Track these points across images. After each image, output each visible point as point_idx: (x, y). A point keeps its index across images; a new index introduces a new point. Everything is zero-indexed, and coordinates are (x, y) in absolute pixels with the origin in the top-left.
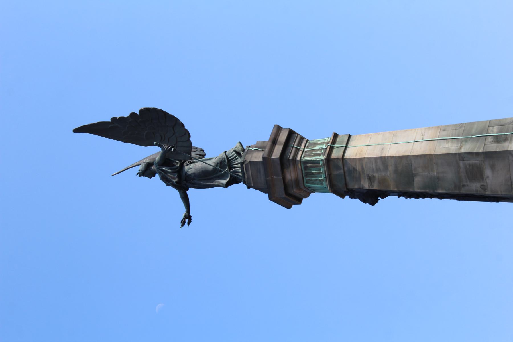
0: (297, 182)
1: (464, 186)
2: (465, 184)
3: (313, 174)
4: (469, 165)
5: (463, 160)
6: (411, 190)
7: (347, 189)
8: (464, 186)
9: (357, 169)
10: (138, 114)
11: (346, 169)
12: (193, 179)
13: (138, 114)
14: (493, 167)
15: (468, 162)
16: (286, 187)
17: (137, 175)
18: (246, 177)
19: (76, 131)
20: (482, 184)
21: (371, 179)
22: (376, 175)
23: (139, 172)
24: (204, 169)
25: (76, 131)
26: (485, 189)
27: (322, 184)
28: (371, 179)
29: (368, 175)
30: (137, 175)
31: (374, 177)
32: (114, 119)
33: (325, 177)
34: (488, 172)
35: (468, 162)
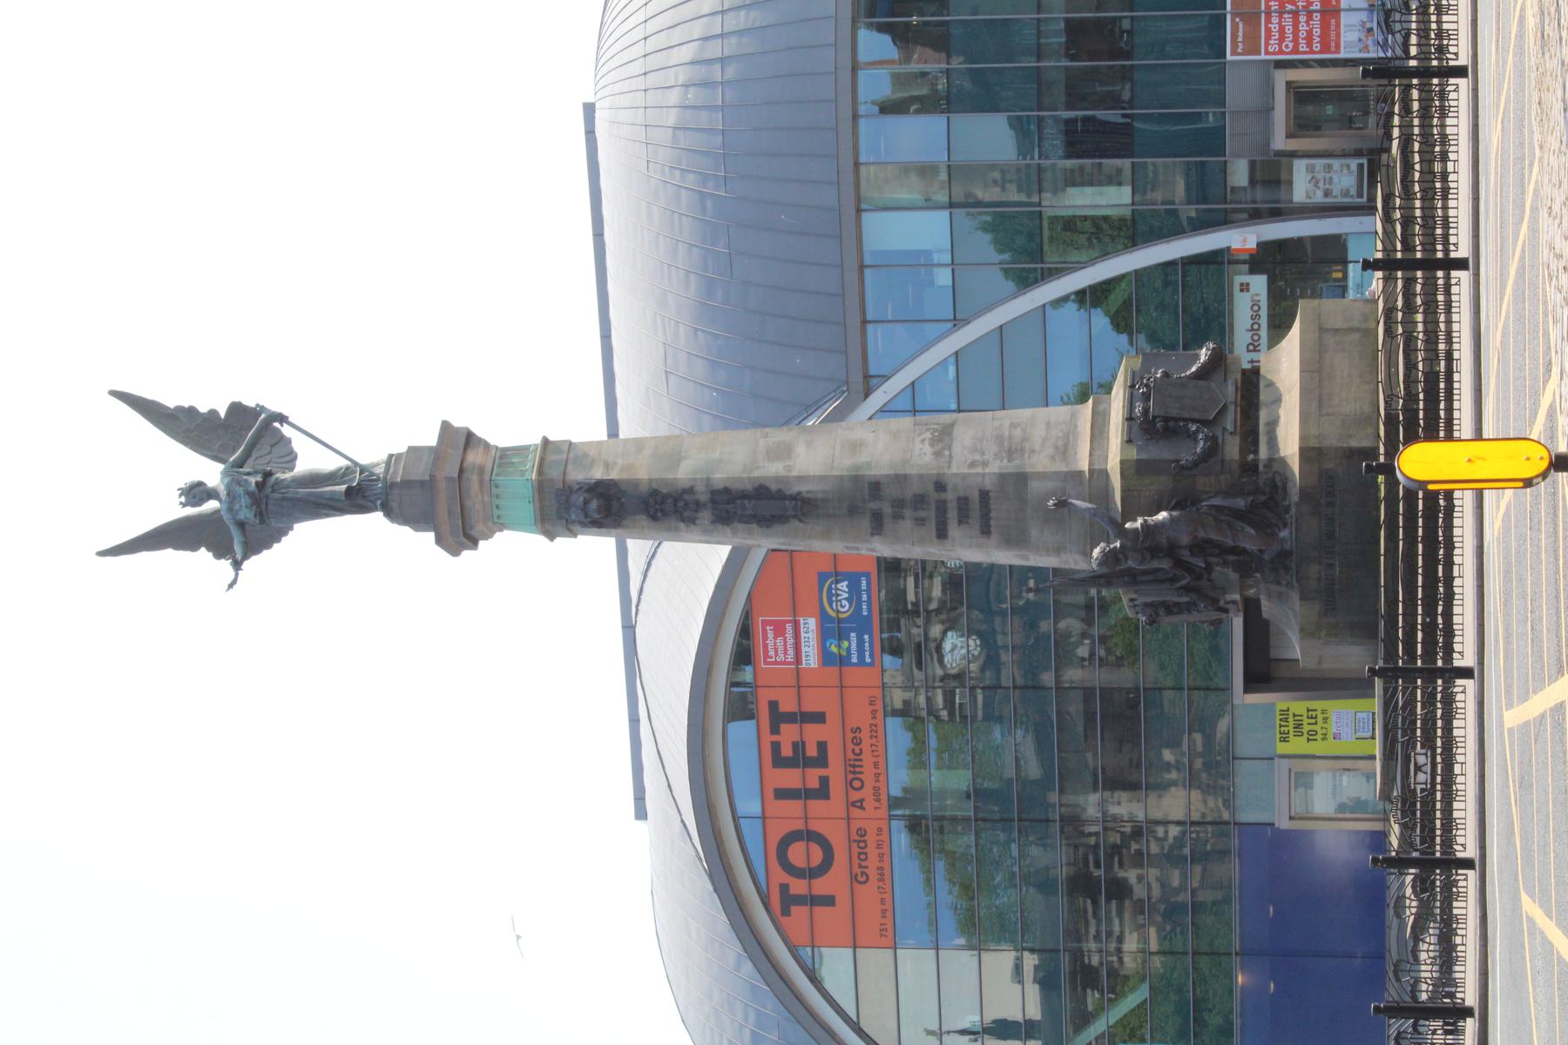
0: (481, 470)
1: (758, 468)
2: (761, 465)
3: (513, 463)
4: (774, 442)
5: (766, 437)
6: (672, 476)
7: (564, 481)
8: (758, 468)
9: (591, 454)
10: (223, 415)
11: (572, 455)
12: (288, 487)
13: (223, 415)
14: (809, 444)
15: (773, 439)
16: (461, 471)
17: (179, 490)
18: (391, 471)
19: (114, 393)
20: (788, 464)
21: (607, 466)
22: (620, 461)
23: (184, 486)
24: (314, 472)
25: (114, 393)
26: (789, 471)
27: (523, 475)
28: (607, 466)
29: (605, 461)
30: (179, 490)
31: (615, 463)
32: (180, 409)
33: (532, 465)
34: (800, 450)
35: (773, 439)
